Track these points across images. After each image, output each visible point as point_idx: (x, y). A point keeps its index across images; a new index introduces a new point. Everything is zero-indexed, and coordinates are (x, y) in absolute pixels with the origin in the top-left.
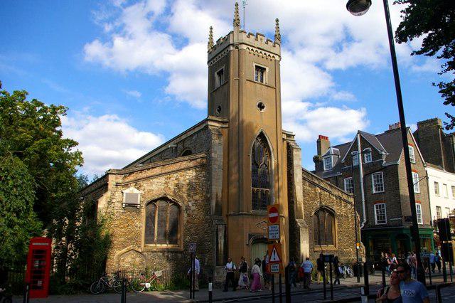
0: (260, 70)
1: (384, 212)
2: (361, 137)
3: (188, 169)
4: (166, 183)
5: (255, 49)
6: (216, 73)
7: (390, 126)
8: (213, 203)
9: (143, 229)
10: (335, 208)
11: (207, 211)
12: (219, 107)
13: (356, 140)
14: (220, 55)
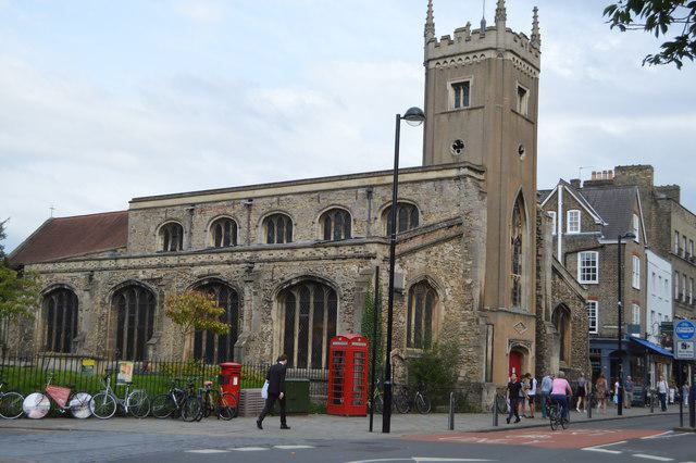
0: (522, 92)
1: (594, 314)
2: (564, 191)
3: (447, 240)
4: (427, 260)
5: (520, 61)
6: (449, 88)
7: (594, 173)
8: (477, 293)
9: (405, 324)
10: (570, 306)
11: (465, 304)
12: (458, 142)
13: (557, 191)
14: (463, 57)
